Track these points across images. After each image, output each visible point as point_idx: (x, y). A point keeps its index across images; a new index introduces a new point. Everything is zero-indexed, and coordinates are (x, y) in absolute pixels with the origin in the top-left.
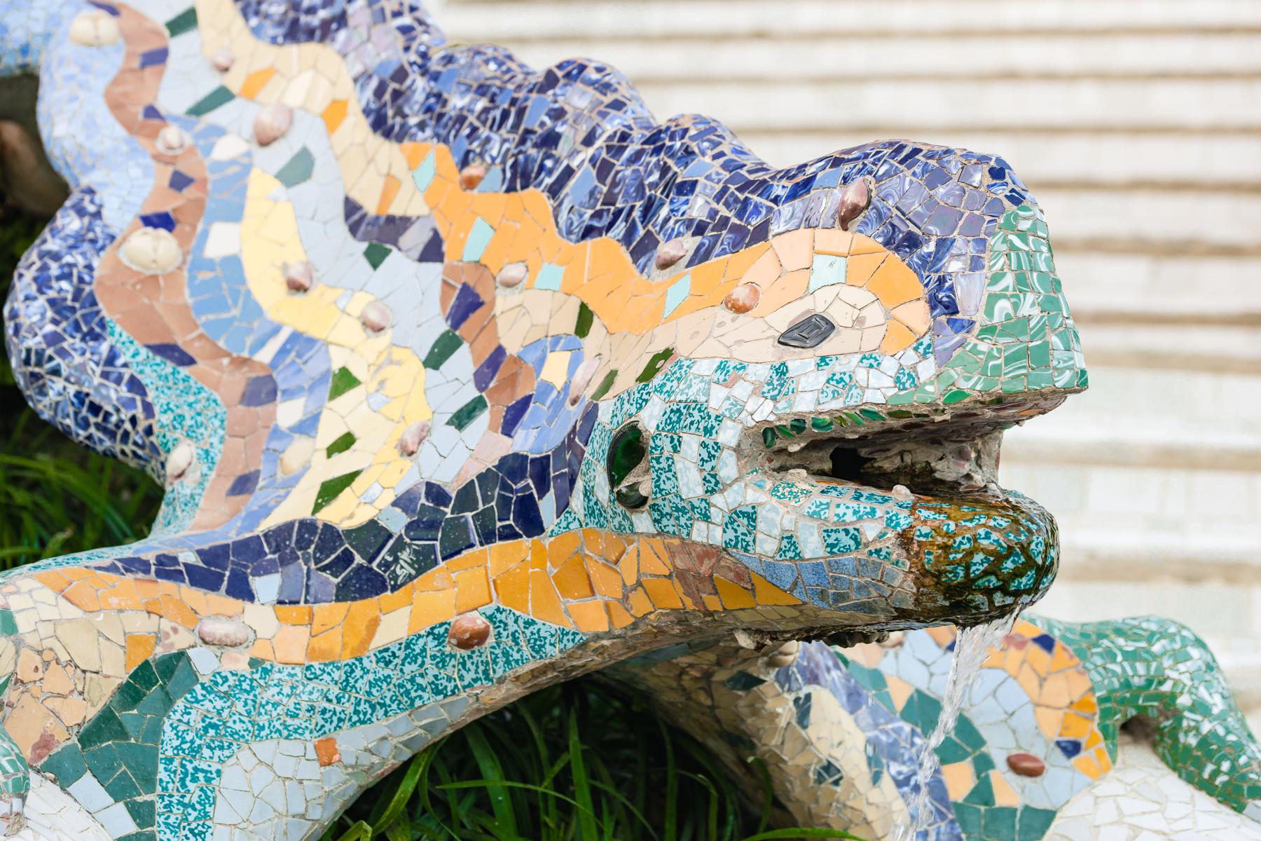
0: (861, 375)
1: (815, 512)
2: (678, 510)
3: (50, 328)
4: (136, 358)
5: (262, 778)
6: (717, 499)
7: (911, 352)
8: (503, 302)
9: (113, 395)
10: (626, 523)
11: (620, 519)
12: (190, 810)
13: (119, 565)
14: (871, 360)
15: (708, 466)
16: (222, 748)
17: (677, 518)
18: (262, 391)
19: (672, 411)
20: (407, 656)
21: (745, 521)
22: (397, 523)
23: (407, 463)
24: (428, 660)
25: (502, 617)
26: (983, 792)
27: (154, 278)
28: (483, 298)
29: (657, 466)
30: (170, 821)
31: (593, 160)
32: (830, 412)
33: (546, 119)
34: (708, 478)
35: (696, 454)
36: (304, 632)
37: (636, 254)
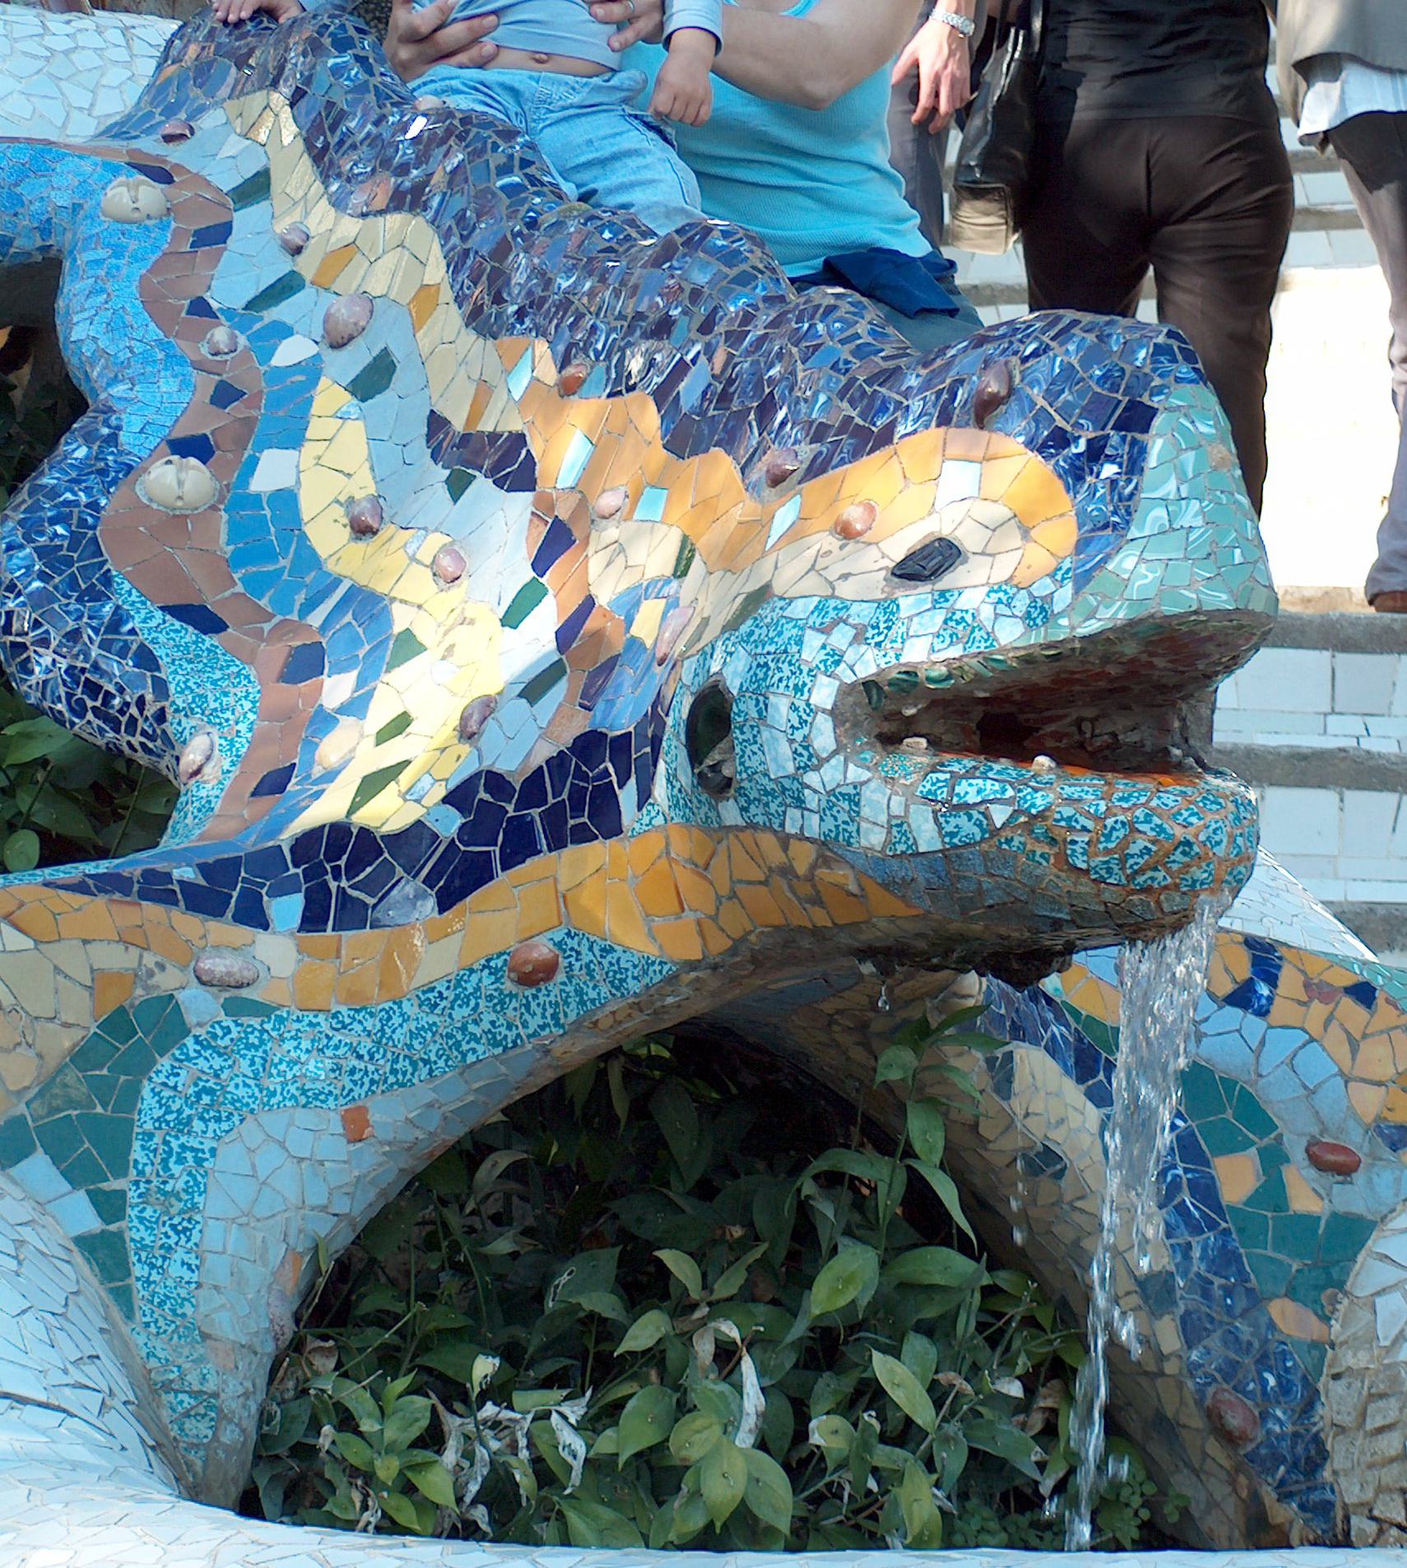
2: (767, 793)
3: (37, 584)
4: (149, 624)
5: (269, 1159)
6: (811, 778)
10: (712, 814)
11: (705, 809)
12: (173, 1200)
13: (90, 882)
16: (218, 1120)
17: (767, 805)
18: (307, 664)
19: (759, 665)
20: (457, 997)
23: (465, 749)
24: (482, 1002)
26: (1272, 1192)
28: (577, 534)
30: (147, 1214)
34: (800, 750)
35: (784, 720)
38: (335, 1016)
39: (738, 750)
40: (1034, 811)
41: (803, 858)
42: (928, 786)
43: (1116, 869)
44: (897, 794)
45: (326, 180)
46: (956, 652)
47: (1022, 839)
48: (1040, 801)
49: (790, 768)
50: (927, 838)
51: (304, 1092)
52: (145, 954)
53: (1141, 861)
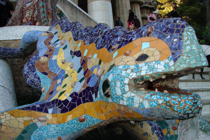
0: (156, 66)
1: (147, 98)
2: (116, 98)
3: (28, 71)
4: (39, 74)
6: (125, 95)
7: (167, 60)
8: (89, 61)
9: (35, 80)
10: (107, 100)
11: (106, 99)
13: (25, 108)
14: (158, 62)
15: (122, 88)
17: (117, 99)
18: (57, 78)
19: (114, 77)
20: (72, 123)
21: (131, 100)
22: (70, 99)
23: (72, 89)
24: (75, 124)
27: (44, 63)
29: (112, 88)
31: (102, 36)
32: (149, 75)
33: (95, 32)
34: (122, 91)
35: (120, 86)
36: (56, 118)
37: (108, 50)
38: (56, 125)
40: (167, 101)
41: (122, 108)
42: (146, 97)
43: (182, 111)
44: (140, 98)
45: (62, 30)
46: (151, 73)
47: (165, 106)
48: (168, 99)
49: (121, 94)
50: (147, 105)
51: (53, 135)
52: (32, 118)
53: (187, 109)
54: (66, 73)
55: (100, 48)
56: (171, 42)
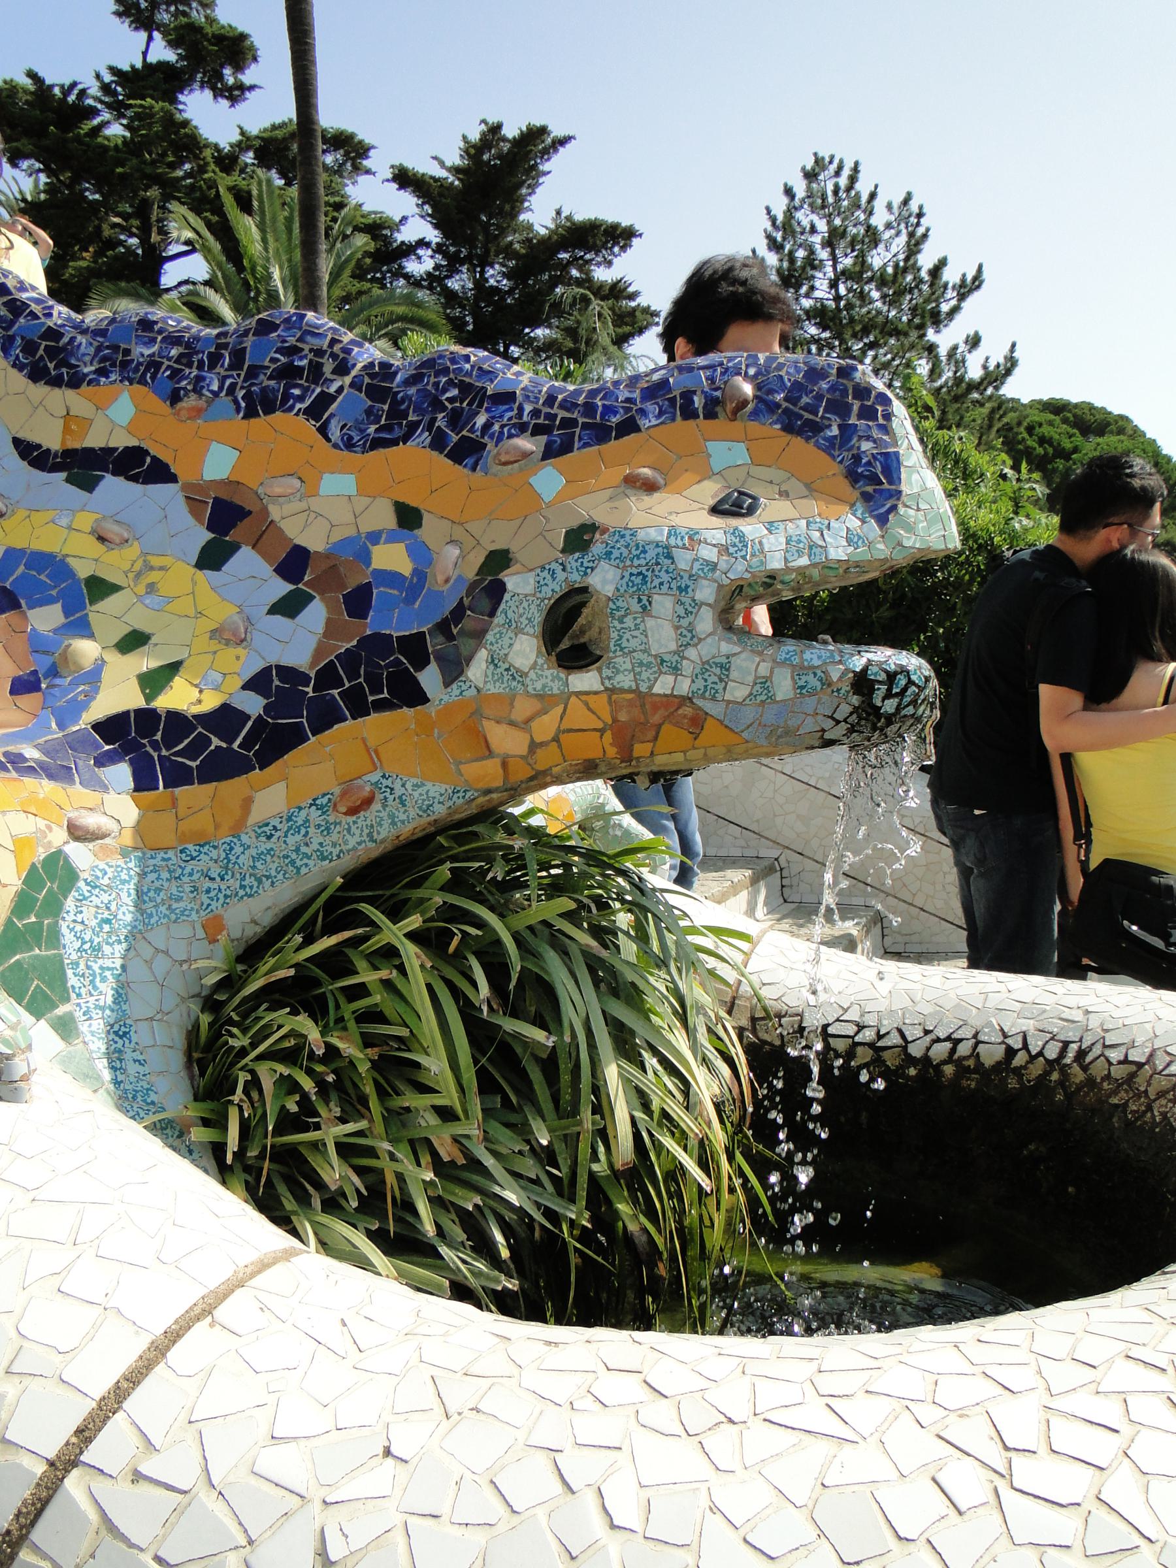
2: (641, 664)
6: (691, 653)
15: (684, 623)
17: (640, 673)
19: (631, 574)
20: (290, 828)
21: (718, 671)
22: (253, 705)
24: (312, 830)
25: (389, 782)
30: (93, 1029)
34: (685, 632)
39: (614, 635)
42: (784, 655)
44: (764, 661)
46: (804, 561)
49: (673, 646)
54: (83, 570)
55: (372, 448)
56: (848, 450)
